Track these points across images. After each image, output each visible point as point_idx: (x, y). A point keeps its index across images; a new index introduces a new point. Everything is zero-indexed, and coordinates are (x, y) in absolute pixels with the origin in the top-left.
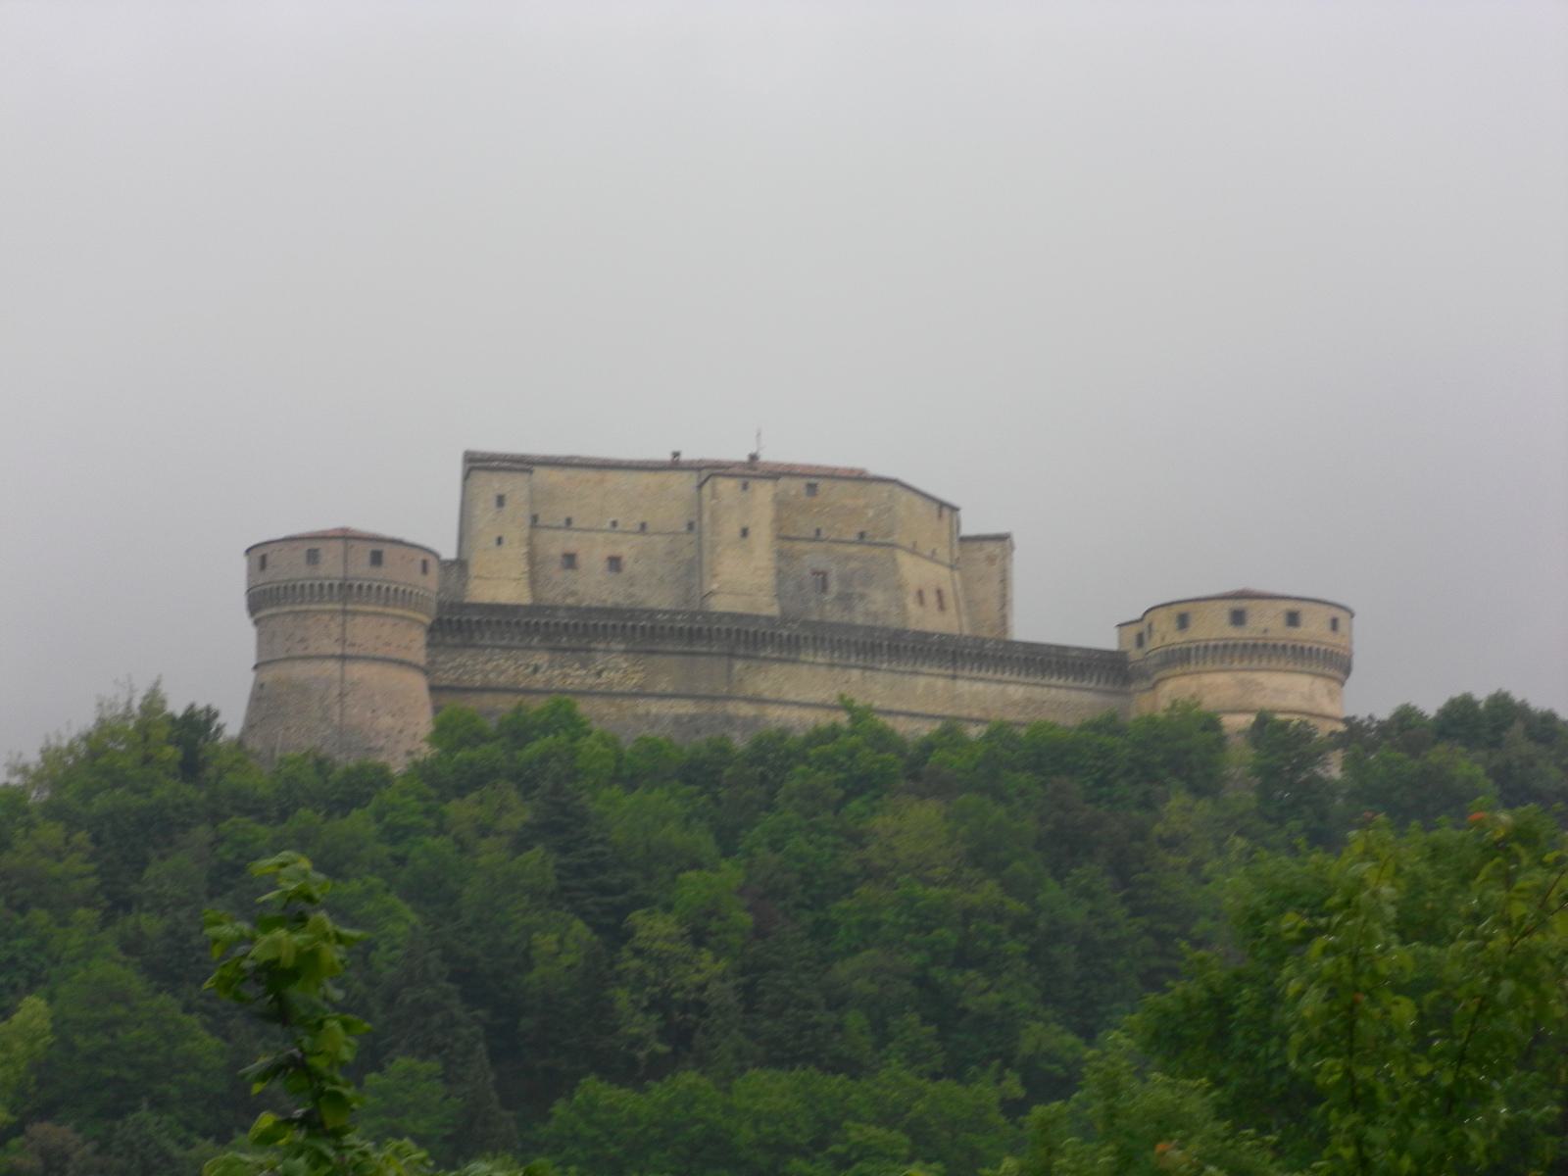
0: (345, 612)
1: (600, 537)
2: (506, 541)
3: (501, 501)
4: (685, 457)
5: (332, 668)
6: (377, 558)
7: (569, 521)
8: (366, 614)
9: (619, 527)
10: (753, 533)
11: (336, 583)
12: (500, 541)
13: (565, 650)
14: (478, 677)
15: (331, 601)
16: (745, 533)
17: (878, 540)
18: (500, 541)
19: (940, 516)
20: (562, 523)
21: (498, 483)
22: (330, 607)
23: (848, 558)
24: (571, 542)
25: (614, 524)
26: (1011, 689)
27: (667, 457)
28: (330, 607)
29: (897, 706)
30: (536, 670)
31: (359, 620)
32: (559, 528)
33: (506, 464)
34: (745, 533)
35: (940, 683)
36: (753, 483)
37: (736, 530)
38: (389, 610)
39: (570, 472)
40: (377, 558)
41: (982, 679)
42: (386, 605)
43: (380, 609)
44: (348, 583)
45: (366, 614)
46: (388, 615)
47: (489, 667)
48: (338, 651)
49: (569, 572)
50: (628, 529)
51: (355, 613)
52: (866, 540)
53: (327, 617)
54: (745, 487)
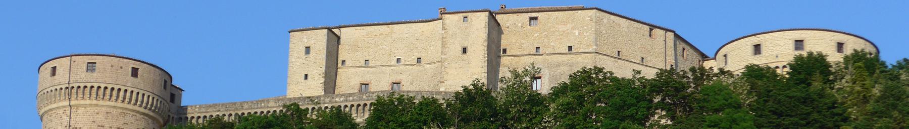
3: (308, 50)
9: (402, 62)
10: (469, 50)
11: (64, 87)
16: (465, 50)
17: (581, 50)
22: (61, 104)
23: (558, 65)
25: (398, 60)
28: (61, 104)
31: (81, 110)
34: (465, 50)
37: (461, 49)
40: (91, 67)
44: (71, 85)
45: (85, 106)
46: (103, 106)
51: (78, 106)
52: (574, 50)
53: (61, 111)
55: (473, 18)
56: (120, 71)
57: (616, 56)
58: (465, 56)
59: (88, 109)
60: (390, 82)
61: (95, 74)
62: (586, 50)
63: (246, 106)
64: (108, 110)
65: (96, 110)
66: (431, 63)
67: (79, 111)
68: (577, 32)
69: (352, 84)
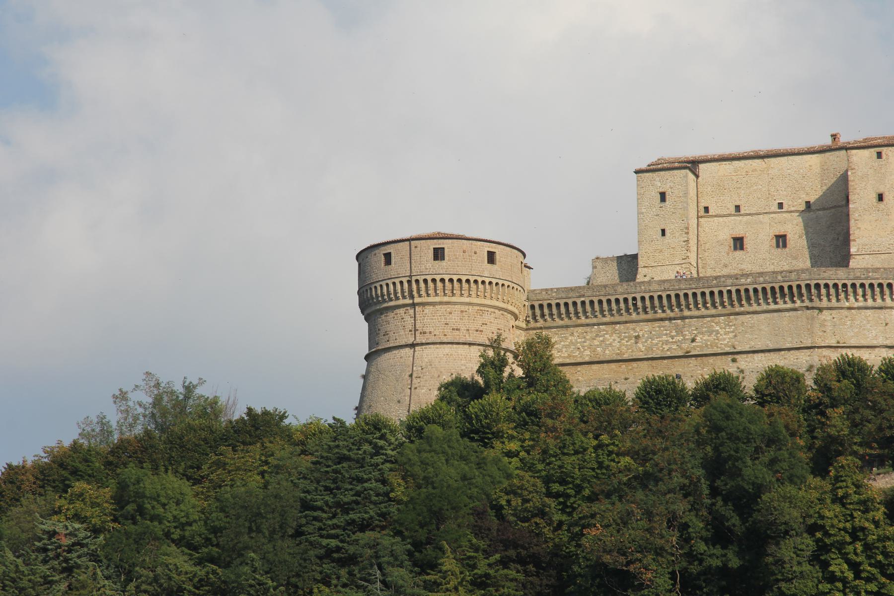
0: (414, 305)
1: (766, 219)
2: (667, 233)
3: (663, 197)
4: (843, 140)
5: (408, 351)
6: (438, 254)
7: (738, 208)
8: (433, 304)
9: (785, 208)
12: (663, 232)
13: (662, 320)
14: (588, 352)
15: (404, 297)
16: (880, 198)
18: (663, 232)
20: (732, 210)
21: (660, 181)
24: (738, 225)
25: (781, 205)
27: (828, 141)
31: (428, 310)
32: (730, 215)
33: (676, 165)
34: (880, 198)
36: (884, 150)
37: (874, 196)
38: (454, 299)
39: (736, 163)
40: (438, 254)
42: (453, 295)
43: (446, 299)
45: (433, 304)
46: (455, 303)
47: (596, 343)
48: (411, 340)
49: (739, 253)
50: (793, 209)
53: (401, 311)
54: (879, 155)
55: (890, 154)
56: (475, 257)
58: (882, 205)
59: (438, 307)
60: (772, 234)
61: (444, 263)
64: (463, 308)
65: (449, 308)
66: (824, 209)
67: (426, 311)
69: (721, 238)
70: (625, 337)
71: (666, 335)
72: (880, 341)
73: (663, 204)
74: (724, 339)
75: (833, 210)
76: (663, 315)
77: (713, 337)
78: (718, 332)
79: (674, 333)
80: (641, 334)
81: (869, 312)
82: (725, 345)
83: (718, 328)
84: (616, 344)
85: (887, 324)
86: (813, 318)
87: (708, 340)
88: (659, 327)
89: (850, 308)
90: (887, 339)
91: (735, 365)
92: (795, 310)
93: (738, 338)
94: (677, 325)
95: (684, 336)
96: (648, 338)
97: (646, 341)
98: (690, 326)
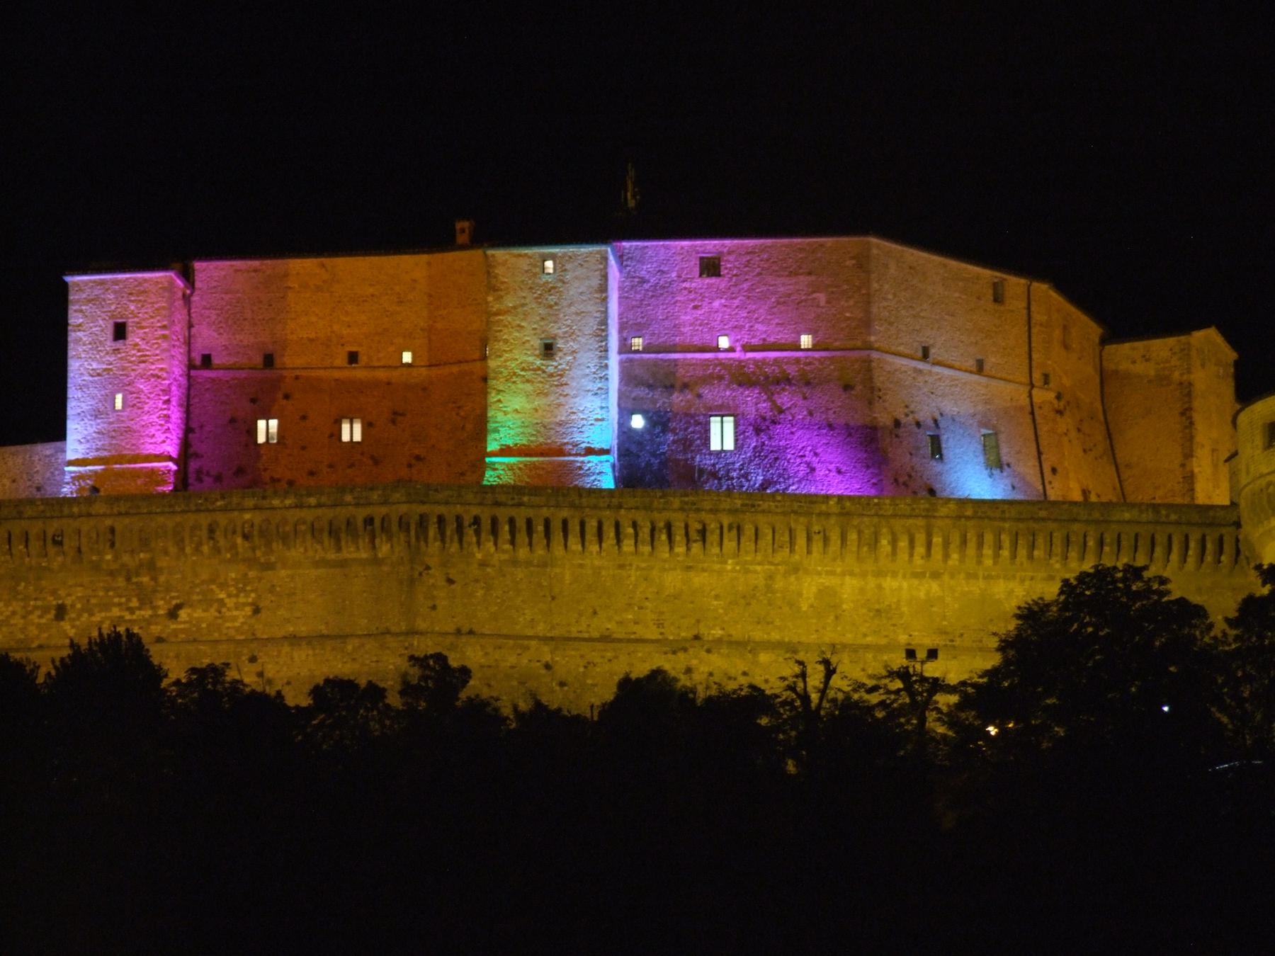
9: (363, 359)
19: (998, 299)
25: (353, 358)
26: (1000, 588)
29: (758, 634)
30: (61, 612)
35: (851, 583)
41: (936, 575)
57: (920, 354)
58: (551, 367)
62: (850, 344)
63: (29, 511)
68: (822, 298)
70: (36, 608)
71: (120, 604)
72: (541, 629)
73: (119, 344)
74: (235, 619)
75: (455, 369)
76: (114, 566)
77: (213, 612)
78: (221, 602)
79: (134, 603)
80: (68, 602)
81: (520, 573)
82: (237, 629)
83: (222, 596)
84: (17, 621)
85: (553, 598)
86: (412, 581)
87: (200, 620)
88: (107, 590)
89: (483, 564)
90: (553, 628)
91: (255, 668)
92: (376, 561)
93: (263, 615)
94: (139, 584)
95: (154, 608)
96: (83, 610)
97: (79, 616)
98: (168, 590)
